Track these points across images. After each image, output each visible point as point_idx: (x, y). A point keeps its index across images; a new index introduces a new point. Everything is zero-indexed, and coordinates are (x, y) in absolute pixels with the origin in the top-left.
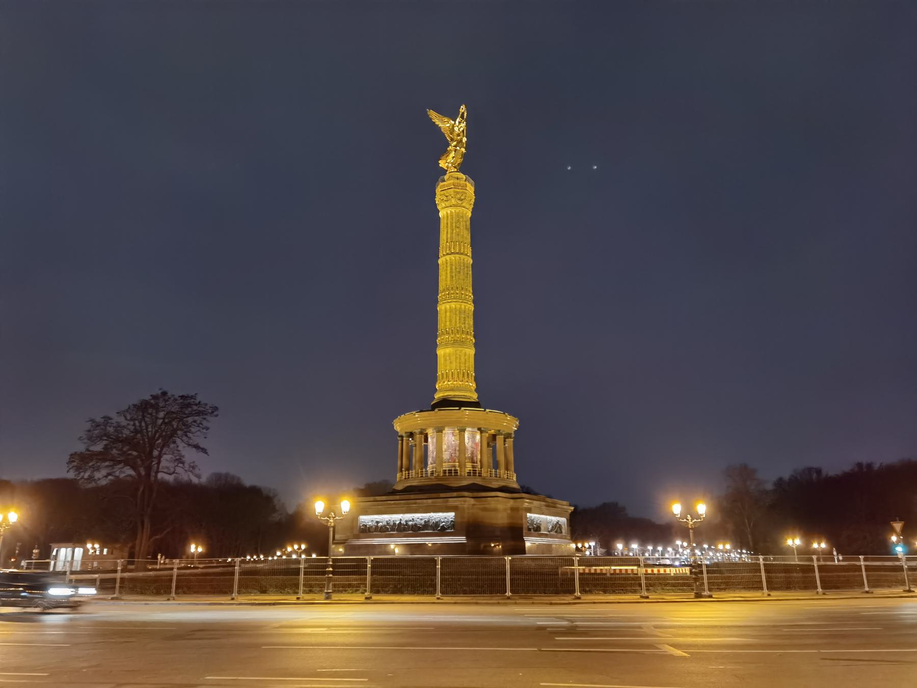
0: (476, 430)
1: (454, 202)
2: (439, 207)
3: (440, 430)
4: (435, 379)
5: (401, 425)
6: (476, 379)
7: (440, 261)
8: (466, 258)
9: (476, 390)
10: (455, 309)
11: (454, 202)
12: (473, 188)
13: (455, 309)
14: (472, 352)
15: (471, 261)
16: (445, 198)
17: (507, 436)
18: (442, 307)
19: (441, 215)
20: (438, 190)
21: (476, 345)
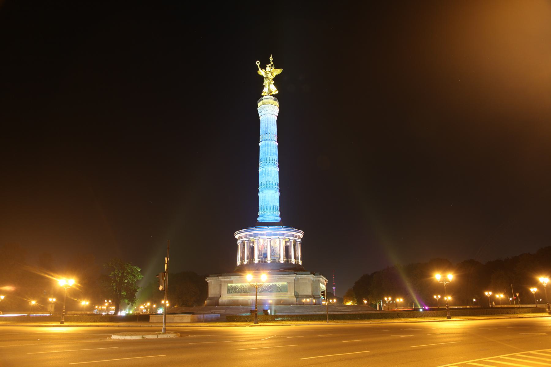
1: (268, 111)
2: (260, 114)
7: (260, 144)
9: (280, 216)
10: (269, 172)
11: (268, 111)
13: (269, 172)
15: (277, 144)
19: (260, 119)
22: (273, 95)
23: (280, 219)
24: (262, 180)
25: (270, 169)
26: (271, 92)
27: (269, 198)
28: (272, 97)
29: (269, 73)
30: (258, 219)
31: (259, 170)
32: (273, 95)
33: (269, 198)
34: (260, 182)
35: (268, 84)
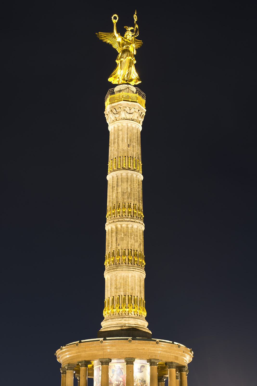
0: (145, 362)
3: (105, 362)
4: (102, 306)
5: (65, 354)
6: (148, 307)
7: (109, 177)
8: (135, 174)
12: (144, 101)
14: (144, 275)
15: (142, 178)
16: (114, 111)
17: (180, 368)
18: (108, 227)
19: (110, 128)
20: (107, 103)
21: (147, 269)
22: (135, 86)
23: (146, 324)
24: (111, 246)
25: (124, 224)
26: (131, 80)
27: (124, 282)
28: (134, 89)
29: (124, 42)
30: (103, 324)
31: (107, 229)
32: (135, 86)
33: (124, 282)
34: (108, 251)
35: (127, 64)
